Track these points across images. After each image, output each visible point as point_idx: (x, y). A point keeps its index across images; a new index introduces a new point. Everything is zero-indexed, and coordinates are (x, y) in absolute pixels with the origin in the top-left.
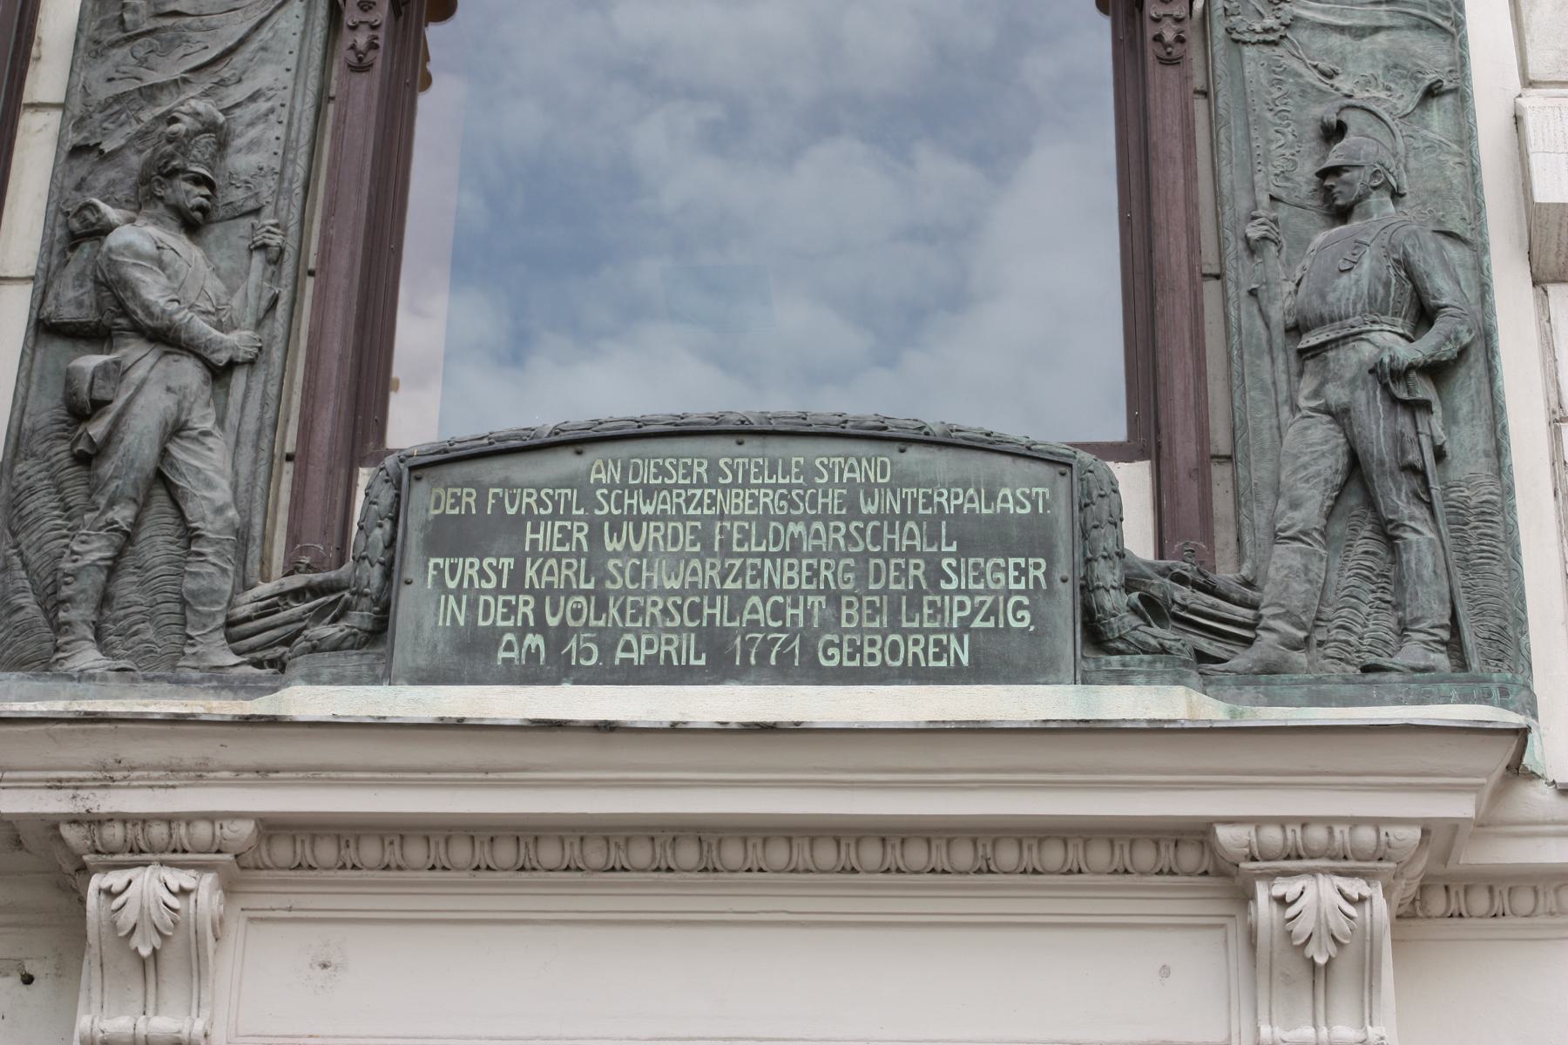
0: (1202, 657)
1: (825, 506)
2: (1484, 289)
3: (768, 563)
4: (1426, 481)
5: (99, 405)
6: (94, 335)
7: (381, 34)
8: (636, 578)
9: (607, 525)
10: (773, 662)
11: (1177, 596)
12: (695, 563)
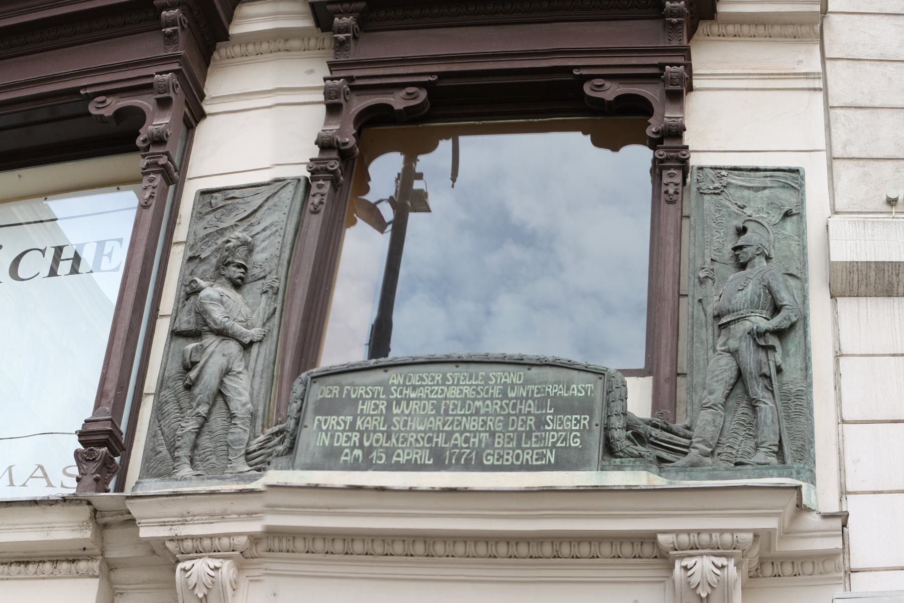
0: (661, 460)
1: (492, 394)
2: (805, 298)
3: (464, 419)
4: (771, 381)
7: (325, 198)
8: (405, 425)
9: (394, 403)
10: (462, 462)
11: (653, 434)
12: (432, 419)
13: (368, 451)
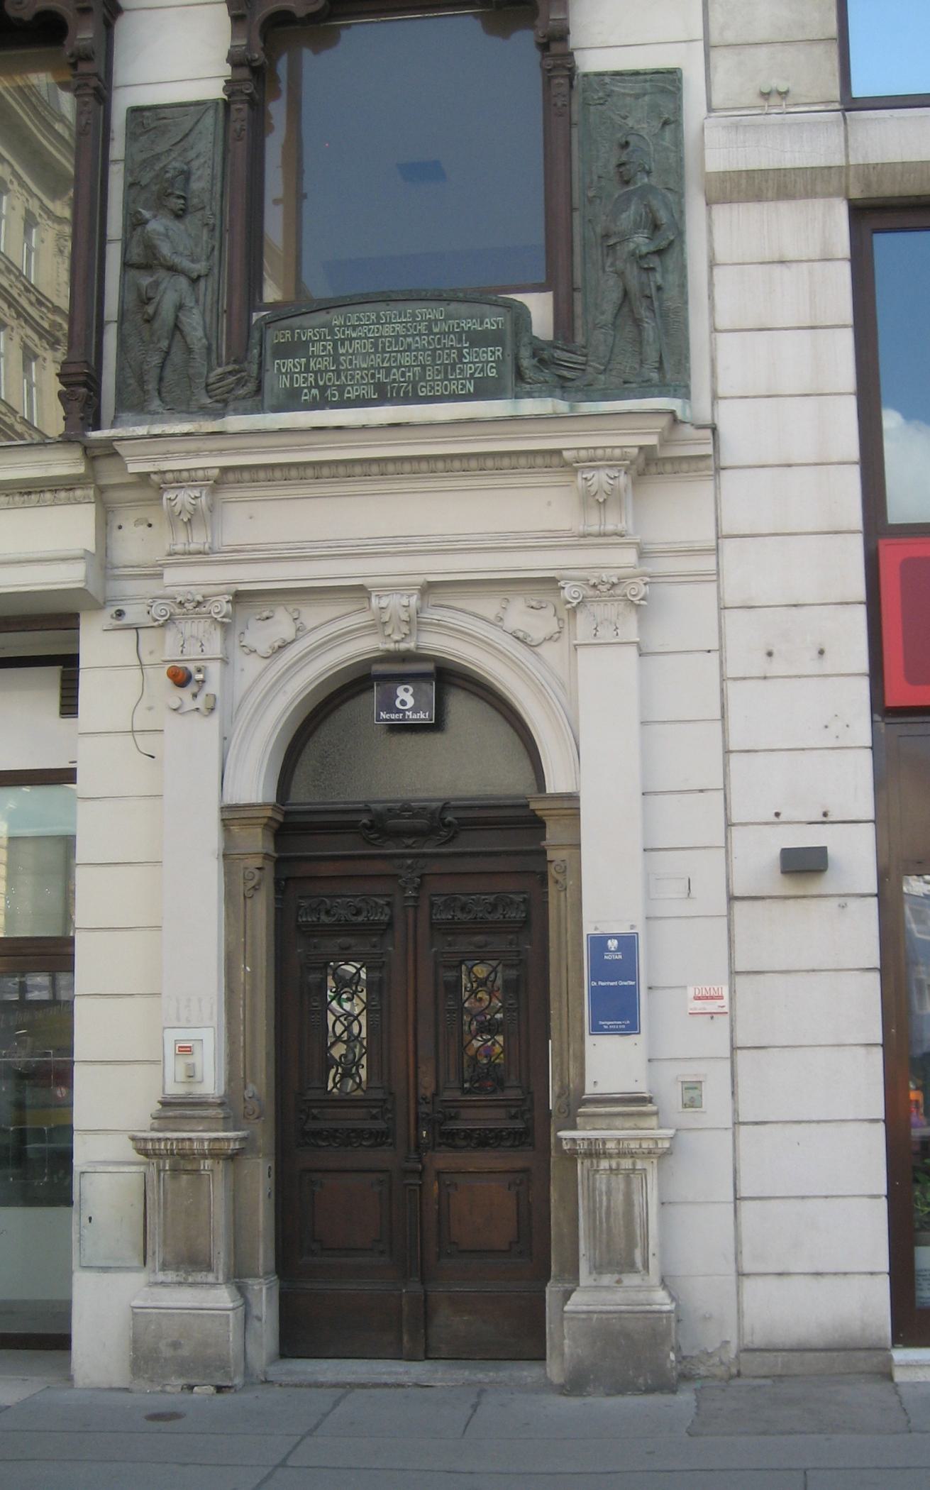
5: (150, 299)
6: (146, 267)
13: (323, 390)
